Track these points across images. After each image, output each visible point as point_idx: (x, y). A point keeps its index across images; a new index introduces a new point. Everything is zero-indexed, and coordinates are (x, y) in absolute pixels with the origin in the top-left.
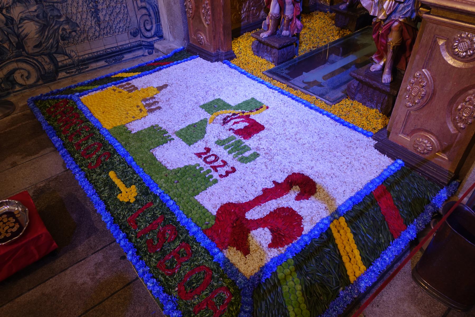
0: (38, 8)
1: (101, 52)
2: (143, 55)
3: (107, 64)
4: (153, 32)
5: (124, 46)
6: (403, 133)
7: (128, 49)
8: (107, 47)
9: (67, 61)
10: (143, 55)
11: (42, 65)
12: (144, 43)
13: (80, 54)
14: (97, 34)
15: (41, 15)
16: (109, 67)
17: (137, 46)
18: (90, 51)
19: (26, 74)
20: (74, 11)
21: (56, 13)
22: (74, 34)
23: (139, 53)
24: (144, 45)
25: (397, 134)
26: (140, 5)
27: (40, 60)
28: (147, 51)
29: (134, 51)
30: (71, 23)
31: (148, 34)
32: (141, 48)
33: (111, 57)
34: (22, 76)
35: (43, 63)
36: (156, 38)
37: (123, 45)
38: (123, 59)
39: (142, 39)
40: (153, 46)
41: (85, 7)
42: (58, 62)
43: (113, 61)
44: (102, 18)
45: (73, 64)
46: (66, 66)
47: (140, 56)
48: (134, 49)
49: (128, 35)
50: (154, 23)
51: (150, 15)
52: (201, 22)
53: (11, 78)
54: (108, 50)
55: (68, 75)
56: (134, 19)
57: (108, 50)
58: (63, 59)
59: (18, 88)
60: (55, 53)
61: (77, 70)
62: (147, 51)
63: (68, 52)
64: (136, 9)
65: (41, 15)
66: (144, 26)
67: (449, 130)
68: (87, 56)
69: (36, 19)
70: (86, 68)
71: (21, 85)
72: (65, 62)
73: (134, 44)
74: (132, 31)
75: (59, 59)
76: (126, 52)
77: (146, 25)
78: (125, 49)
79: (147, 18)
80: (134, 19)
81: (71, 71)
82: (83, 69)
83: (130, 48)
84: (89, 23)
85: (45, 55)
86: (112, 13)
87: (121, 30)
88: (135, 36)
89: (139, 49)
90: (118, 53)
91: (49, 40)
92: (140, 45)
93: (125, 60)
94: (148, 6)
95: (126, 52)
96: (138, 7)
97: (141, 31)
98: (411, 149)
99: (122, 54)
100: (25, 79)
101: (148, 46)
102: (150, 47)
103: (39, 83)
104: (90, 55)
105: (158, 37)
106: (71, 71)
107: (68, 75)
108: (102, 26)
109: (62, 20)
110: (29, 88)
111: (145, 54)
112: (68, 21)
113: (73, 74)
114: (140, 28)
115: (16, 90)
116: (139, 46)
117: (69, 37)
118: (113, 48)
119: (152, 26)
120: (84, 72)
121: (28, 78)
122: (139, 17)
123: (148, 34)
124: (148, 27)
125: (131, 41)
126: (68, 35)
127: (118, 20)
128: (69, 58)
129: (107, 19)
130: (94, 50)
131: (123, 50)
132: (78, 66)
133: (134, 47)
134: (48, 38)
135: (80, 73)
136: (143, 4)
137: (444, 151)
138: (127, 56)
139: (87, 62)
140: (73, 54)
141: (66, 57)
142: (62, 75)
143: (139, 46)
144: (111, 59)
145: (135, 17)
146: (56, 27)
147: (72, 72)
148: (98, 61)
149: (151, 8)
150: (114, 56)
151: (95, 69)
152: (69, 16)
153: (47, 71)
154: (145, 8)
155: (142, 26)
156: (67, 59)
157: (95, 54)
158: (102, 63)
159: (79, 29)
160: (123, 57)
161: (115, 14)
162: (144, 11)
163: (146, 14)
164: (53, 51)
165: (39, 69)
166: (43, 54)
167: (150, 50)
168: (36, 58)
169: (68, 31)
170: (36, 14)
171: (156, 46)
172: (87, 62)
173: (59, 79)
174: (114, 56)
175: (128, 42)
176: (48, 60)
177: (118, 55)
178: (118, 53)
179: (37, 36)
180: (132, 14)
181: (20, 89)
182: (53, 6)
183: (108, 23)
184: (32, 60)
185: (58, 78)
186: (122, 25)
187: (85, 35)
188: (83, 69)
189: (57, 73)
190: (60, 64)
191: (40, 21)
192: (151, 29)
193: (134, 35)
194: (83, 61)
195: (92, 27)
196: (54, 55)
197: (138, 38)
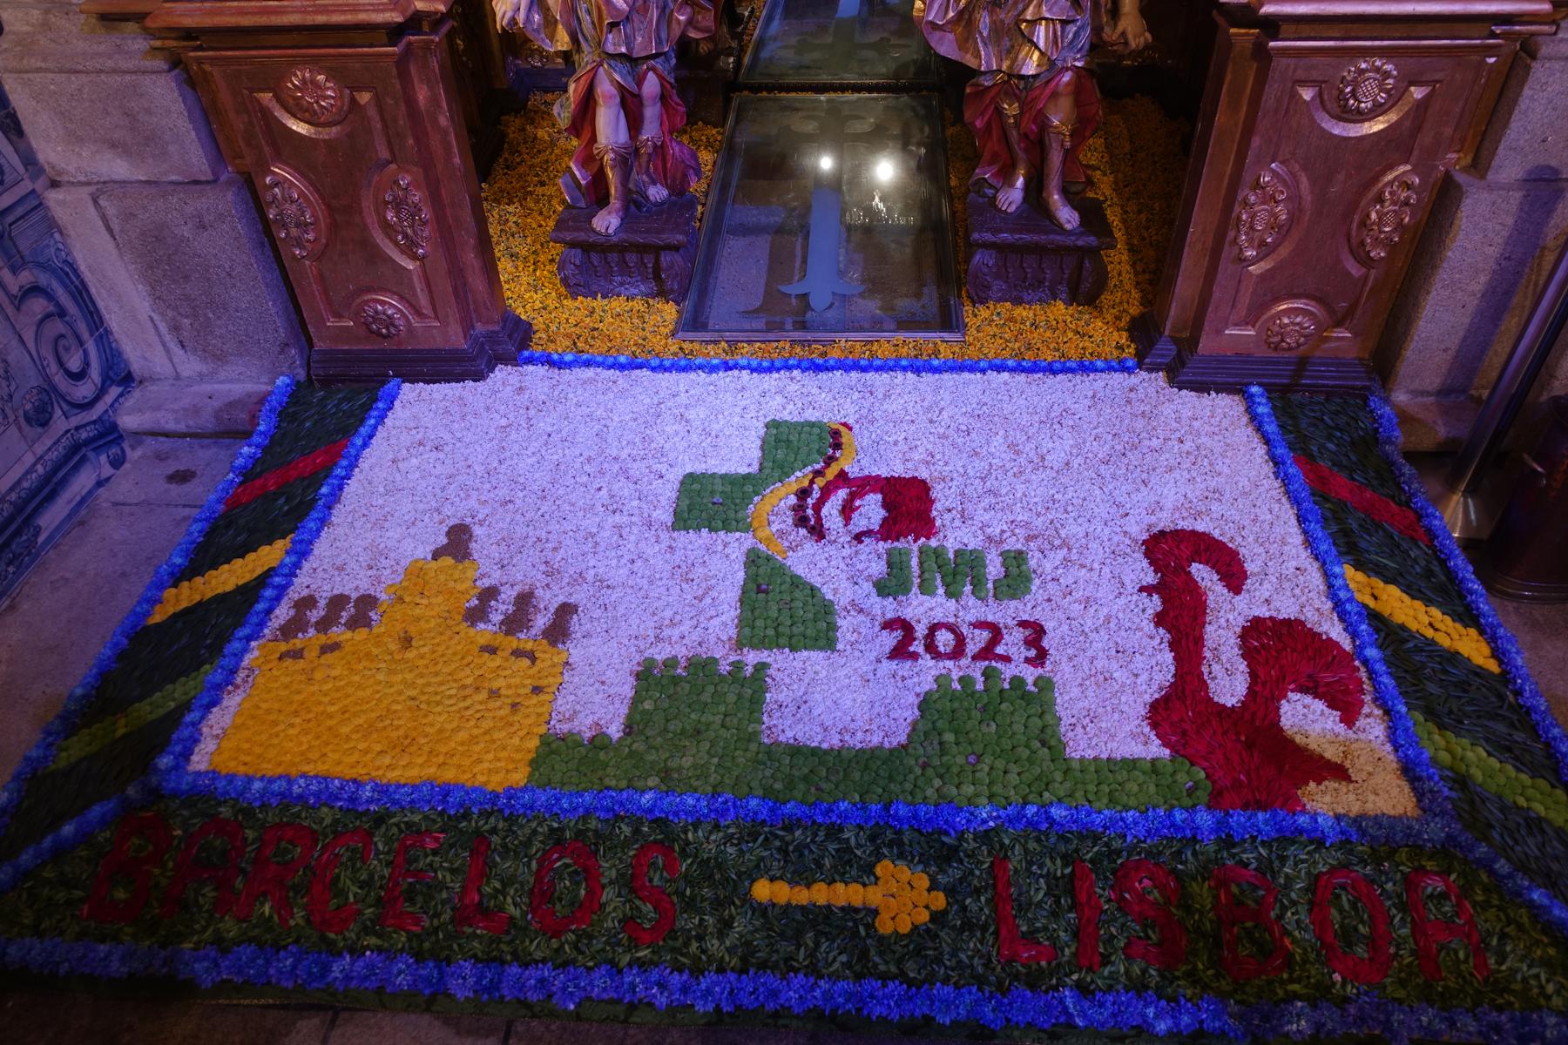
2: (100, 484)
4: (95, 373)
5: (26, 484)
10: (100, 484)
12: (84, 435)
17: (67, 458)
23: (83, 481)
25: (1219, 332)
26: (14, 290)
28: (103, 458)
29: (64, 482)
31: (84, 391)
32: (84, 459)
36: (115, 391)
37: (19, 482)
38: (41, 539)
39: (75, 421)
40: (114, 427)
43: (11, 569)
47: (90, 492)
48: (61, 474)
49: (20, 429)
50: (85, 335)
51: (62, 313)
52: (374, 256)
62: (103, 458)
64: (10, 310)
66: (61, 363)
67: (1349, 274)
73: (54, 455)
74: (28, 406)
77: (65, 359)
78: (33, 493)
79: (57, 327)
83: (46, 479)
88: (44, 424)
89: (76, 468)
90: (13, 527)
92: (76, 448)
93: (50, 538)
94: (43, 279)
96: (12, 297)
97: (55, 389)
98: (1264, 352)
101: (101, 435)
102: (109, 436)
105: (119, 385)
111: (104, 475)
114: (47, 378)
116: (74, 455)
119: (86, 353)
122: (29, 336)
123: (84, 391)
124: (74, 364)
125: (40, 449)
131: (26, 502)
133: (57, 467)
136: (26, 277)
138: (50, 518)
143: (74, 455)
145: (15, 342)
149: (55, 284)
154: (35, 290)
155: (53, 368)
162: (38, 306)
163: (48, 316)
167: (114, 450)
171: (129, 421)
175: (29, 459)
177: (18, 533)
178: (13, 527)
192: (87, 364)
193: (40, 417)
197: (60, 424)
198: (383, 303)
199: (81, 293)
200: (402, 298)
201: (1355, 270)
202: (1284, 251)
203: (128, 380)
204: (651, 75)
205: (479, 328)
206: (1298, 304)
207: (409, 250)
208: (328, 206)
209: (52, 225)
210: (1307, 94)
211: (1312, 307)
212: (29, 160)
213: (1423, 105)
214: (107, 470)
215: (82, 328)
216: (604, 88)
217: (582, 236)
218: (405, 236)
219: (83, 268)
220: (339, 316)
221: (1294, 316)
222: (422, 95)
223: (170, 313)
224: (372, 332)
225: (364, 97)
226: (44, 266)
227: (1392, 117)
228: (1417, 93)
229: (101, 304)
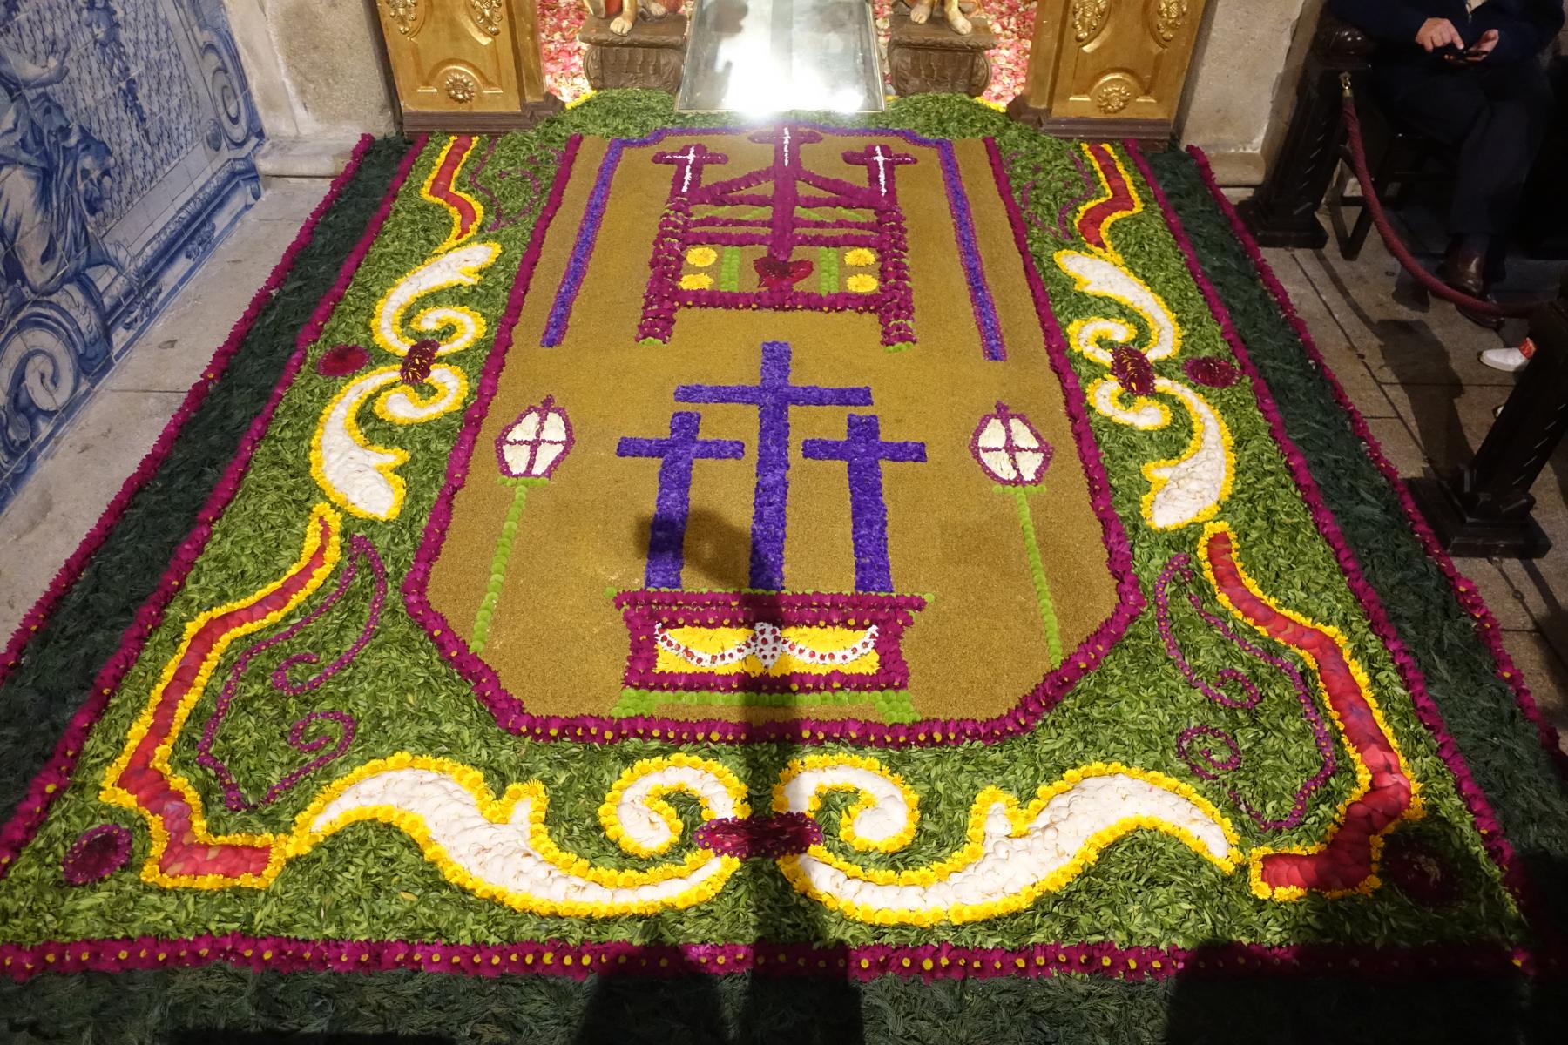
0: (18, 112)
1: (172, 227)
3: (190, 263)
6: (1077, 94)
7: (215, 196)
8: (179, 203)
9: (117, 285)
10: (248, 207)
11: (73, 321)
13: (135, 249)
14: (150, 167)
15: (29, 138)
16: (199, 272)
18: (151, 232)
19: (49, 371)
20: (90, 102)
21: (58, 122)
22: (106, 179)
23: (236, 202)
24: (241, 173)
25: (1065, 98)
27: (64, 305)
30: (93, 147)
31: (238, 132)
33: (192, 237)
34: (43, 376)
35: (73, 313)
36: (254, 141)
38: (216, 234)
40: (253, 168)
41: (107, 80)
42: (101, 295)
44: (146, 108)
45: (131, 292)
46: (118, 305)
51: (226, 71)
52: (457, 34)
53: (23, 400)
54: (183, 214)
55: (132, 333)
56: (202, 91)
57: (183, 214)
58: (109, 280)
59: (45, 428)
60: (89, 265)
61: (143, 308)
63: (111, 250)
65: (29, 138)
68: (149, 251)
69: (24, 156)
70: (158, 293)
71: (49, 414)
72: (114, 291)
73: (223, 174)
75: (101, 285)
76: (214, 210)
79: (222, 79)
80: (202, 91)
81: (133, 316)
82: (152, 300)
83: (219, 190)
84: (125, 135)
85: (70, 281)
86: (159, 84)
87: (189, 135)
88: (217, 149)
91: (65, 224)
92: (233, 174)
94: (216, 41)
95: (214, 210)
99: (210, 216)
100: (51, 387)
102: (250, 174)
103: (83, 389)
104: (155, 245)
106: (133, 316)
107: (132, 333)
108: (153, 139)
109: (73, 140)
110: (68, 416)
112: (86, 134)
113: (139, 324)
115: (42, 437)
117: (100, 199)
118: (188, 203)
120: (157, 311)
121: (54, 382)
124: (232, 111)
126: (96, 194)
127: (175, 102)
128: (120, 274)
129: (156, 109)
130: (159, 226)
132: (141, 292)
134: (62, 218)
135: (151, 316)
136: (204, 37)
137: (1147, 93)
138: (221, 220)
139: (154, 271)
140: (122, 254)
141: (113, 272)
142: (120, 336)
144: (195, 243)
146: (68, 171)
147: (135, 320)
148: (171, 261)
150: (197, 230)
151: (175, 289)
152: (86, 126)
153: (87, 338)
154: (210, 47)
155: (221, 109)
156: (115, 279)
157: (163, 237)
158: (182, 265)
159: (112, 161)
160: (214, 229)
161: (164, 86)
162: (212, 58)
163: (218, 69)
164: (83, 261)
165: (70, 337)
166: (65, 280)
167: (254, 185)
168: (53, 298)
169: (95, 174)
170: (18, 137)
171: (264, 166)
172: (154, 271)
173: (117, 357)
174: (197, 230)
175: (209, 172)
176: (79, 297)
177: (203, 224)
179: (38, 219)
180: (194, 76)
181: (50, 429)
182: (45, 94)
183: (161, 120)
184: (47, 312)
185: (115, 351)
186: (186, 119)
187: (129, 180)
188: (152, 300)
189: (107, 333)
190: (107, 301)
191: (34, 163)
194: (146, 271)
195: (135, 144)
196: (88, 272)
197: (227, 153)
198: (461, 73)
199: (235, 57)
200: (476, 69)
201: (1155, 49)
202: (1105, 34)
203: (261, 134)
206: (1117, 76)
211: (1128, 78)
214: (251, 200)
215: (236, 84)
217: (602, 37)
218: (483, 16)
219: (237, 38)
220: (427, 84)
221: (1113, 85)
223: (299, 78)
226: (216, 30)
229: (247, 71)
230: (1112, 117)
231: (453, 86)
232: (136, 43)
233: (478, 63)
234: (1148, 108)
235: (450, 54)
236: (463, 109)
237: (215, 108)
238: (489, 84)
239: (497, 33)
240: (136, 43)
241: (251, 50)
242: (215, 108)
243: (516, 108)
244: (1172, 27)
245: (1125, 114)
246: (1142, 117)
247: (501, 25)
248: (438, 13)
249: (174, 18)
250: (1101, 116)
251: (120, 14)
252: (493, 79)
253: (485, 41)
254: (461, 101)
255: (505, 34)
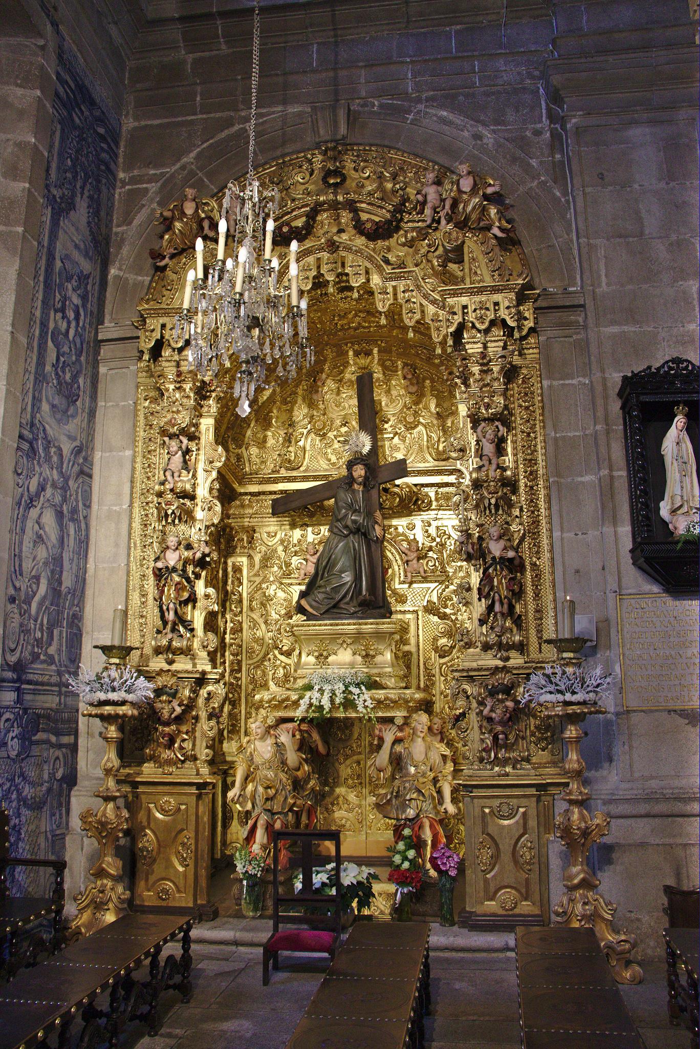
6: (488, 900)
25: (482, 903)
52: (169, 865)
56: (42, 880)
122: (47, 876)
137: (526, 899)
200: (174, 883)
204: (278, 822)
205: (199, 902)
207: (183, 861)
208: (159, 845)
209: (64, 846)
210: (487, 811)
211: (513, 891)
212: (67, 824)
213: (524, 814)
216: (261, 823)
220: (149, 890)
221: (507, 895)
222: (201, 809)
224: (160, 898)
225: (183, 807)
227: (517, 818)
228: (522, 810)
230: (511, 913)
231: (162, 891)
232: (24, 850)
233: (176, 881)
234: (526, 907)
235: (163, 875)
236: (164, 904)
237: (45, 890)
238: (179, 891)
239: (187, 865)
240: (24, 850)
241: (70, 870)
242: (45, 890)
243: (191, 905)
244: (528, 864)
245: (517, 911)
246: (526, 912)
247: (191, 862)
248: (161, 855)
249: (43, 846)
250: (504, 913)
251: (23, 835)
252: (182, 890)
253: (181, 869)
254: (164, 900)
255: (192, 866)
